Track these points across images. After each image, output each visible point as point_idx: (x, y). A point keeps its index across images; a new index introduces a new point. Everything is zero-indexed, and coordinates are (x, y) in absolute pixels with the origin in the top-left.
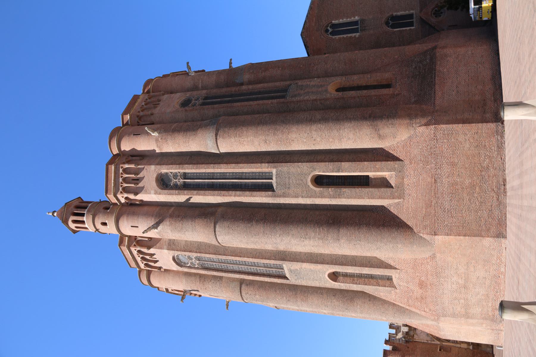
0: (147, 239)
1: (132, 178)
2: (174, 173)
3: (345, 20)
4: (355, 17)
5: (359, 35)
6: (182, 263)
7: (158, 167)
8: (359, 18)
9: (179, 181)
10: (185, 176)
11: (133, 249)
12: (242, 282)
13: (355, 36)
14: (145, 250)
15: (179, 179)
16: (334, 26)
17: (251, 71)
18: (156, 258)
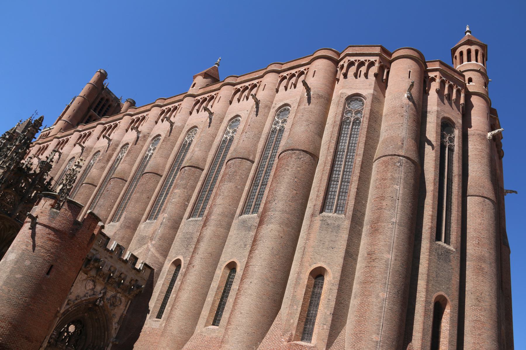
0: (384, 77)
1: (451, 94)
2: (454, 140)
6: (351, 102)
7: (460, 128)
9: (447, 141)
10: (451, 150)
11: (377, 58)
12: (314, 157)
14: (374, 70)
15: (449, 143)
18: (360, 77)
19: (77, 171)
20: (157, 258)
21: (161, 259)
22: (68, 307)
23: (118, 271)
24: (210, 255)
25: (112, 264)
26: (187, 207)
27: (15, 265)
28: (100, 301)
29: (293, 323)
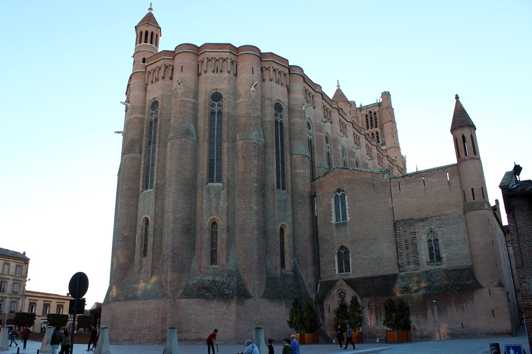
3: (347, 207)
4: (349, 216)
5: (332, 223)
8: (348, 221)
13: (332, 219)
16: (343, 196)
17: (244, 145)
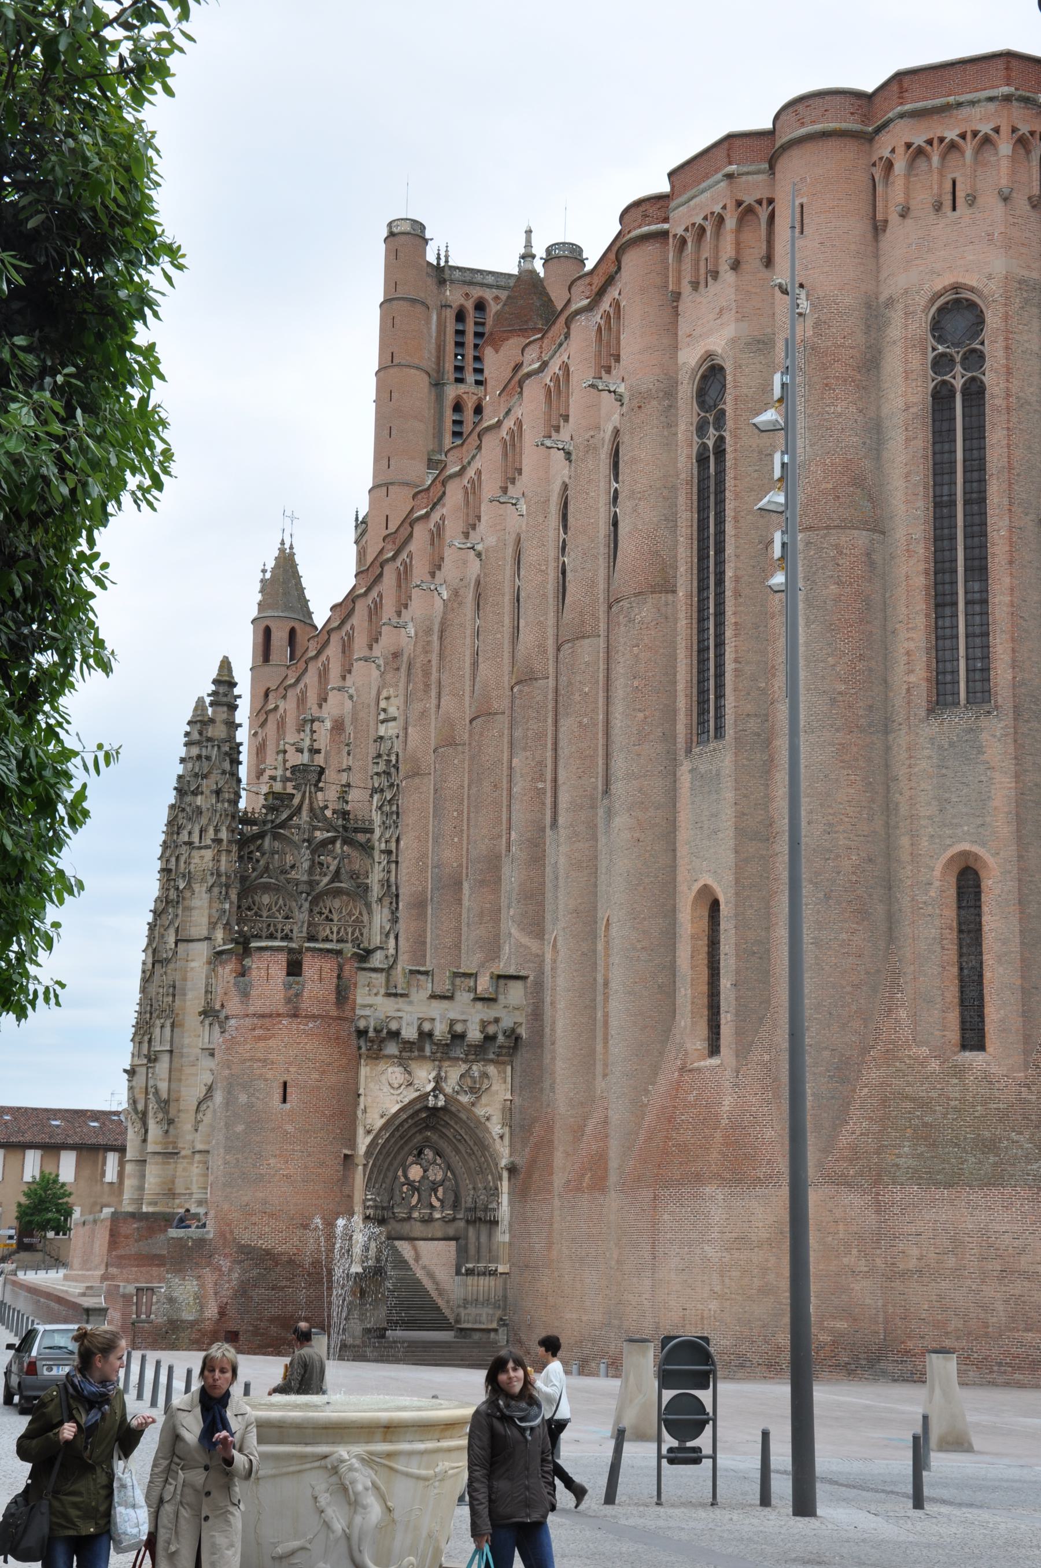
19: (391, 738)
20: (526, 947)
21: (534, 945)
22: (369, 1139)
23: (441, 1022)
24: (575, 915)
25: (421, 1016)
26: (544, 793)
27: (227, 1111)
28: (436, 1097)
29: (685, 1028)
